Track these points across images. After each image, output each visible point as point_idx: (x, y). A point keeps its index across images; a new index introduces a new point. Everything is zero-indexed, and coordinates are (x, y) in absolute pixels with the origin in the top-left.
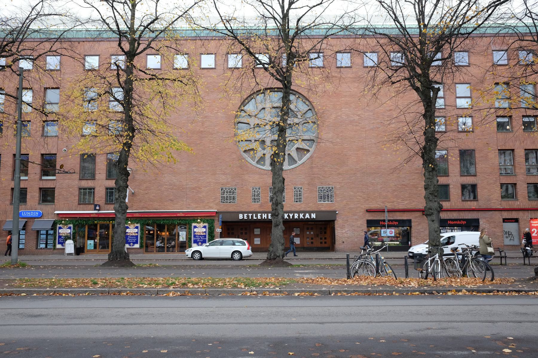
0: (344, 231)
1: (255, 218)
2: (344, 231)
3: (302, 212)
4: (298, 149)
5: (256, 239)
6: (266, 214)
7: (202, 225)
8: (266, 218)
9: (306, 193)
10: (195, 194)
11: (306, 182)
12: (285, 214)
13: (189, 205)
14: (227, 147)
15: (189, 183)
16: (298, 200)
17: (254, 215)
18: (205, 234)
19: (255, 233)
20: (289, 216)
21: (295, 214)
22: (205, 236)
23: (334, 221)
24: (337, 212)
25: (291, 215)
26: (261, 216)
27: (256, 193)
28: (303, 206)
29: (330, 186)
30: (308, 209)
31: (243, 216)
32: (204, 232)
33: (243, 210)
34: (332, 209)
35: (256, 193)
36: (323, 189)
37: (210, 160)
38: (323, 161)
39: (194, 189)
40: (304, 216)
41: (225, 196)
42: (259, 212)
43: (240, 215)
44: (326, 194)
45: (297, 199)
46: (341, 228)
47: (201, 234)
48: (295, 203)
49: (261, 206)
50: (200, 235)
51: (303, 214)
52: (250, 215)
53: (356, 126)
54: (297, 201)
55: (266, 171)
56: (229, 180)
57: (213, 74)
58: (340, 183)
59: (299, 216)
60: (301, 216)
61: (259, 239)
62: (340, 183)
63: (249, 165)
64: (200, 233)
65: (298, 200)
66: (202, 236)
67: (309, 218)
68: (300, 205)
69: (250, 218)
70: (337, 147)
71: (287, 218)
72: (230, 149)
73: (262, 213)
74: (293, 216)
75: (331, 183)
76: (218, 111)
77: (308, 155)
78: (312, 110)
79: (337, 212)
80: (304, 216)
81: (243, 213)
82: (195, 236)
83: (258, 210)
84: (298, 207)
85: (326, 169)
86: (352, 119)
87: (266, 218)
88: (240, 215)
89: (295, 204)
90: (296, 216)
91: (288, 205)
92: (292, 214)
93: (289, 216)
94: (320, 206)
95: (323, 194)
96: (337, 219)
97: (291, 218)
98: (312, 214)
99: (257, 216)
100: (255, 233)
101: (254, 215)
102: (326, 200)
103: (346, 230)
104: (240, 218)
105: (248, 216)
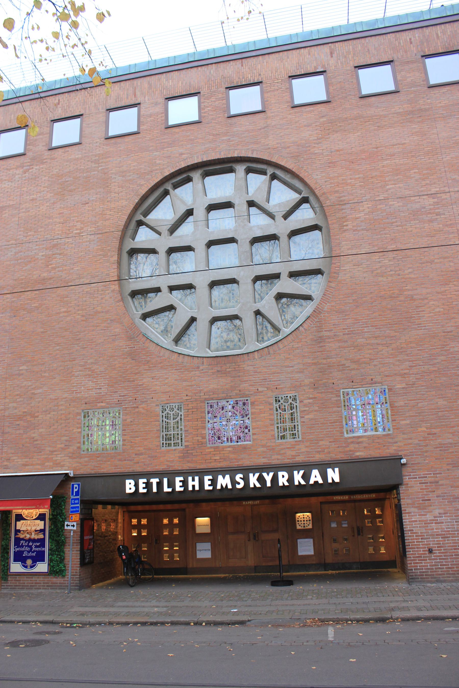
0: (429, 517)
1: (166, 489)
2: (429, 517)
3: (298, 467)
4: (279, 296)
5: (200, 546)
6: (197, 478)
7: (35, 512)
8: (197, 488)
9: (308, 413)
10: (21, 432)
11: (307, 381)
12: (251, 475)
13: (8, 460)
14: (99, 309)
15: (11, 405)
17: (165, 481)
18: (41, 536)
20: (261, 479)
21: (280, 474)
22: (42, 541)
23: (396, 487)
24: (403, 461)
25: (268, 478)
26: (185, 483)
28: (304, 449)
30: (318, 458)
31: (137, 485)
32: (41, 531)
33: (138, 469)
37: (58, 344)
38: (349, 321)
39: (20, 418)
40: (306, 477)
42: (179, 474)
43: (128, 481)
45: (285, 430)
46: (419, 508)
47: (34, 536)
48: (280, 441)
49: (186, 454)
50: (30, 540)
51: (302, 472)
52: (154, 481)
53: (431, 221)
54: (283, 437)
56: (104, 390)
57: (75, 153)
58: (403, 375)
59: (291, 479)
60: (298, 478)
61: (208, 546)
62: (403, 375)
63: (152, 347)
64: (30, 533)
66: (34, 541)
67: (321, 481)
68: (292, 447)
69: (155, 490)
70: (384, 279)
71: (258, 485)
72: (107, 312)
73: (186, 474)
74: (275, 479)
75: (378, 378)
76: (82, 228)
78: (311, 199)
79: (403, 461)
80: (306, 477)
81: (136, 476)
82: (18, 541)
83: (178, 466)
84: (290, 453)
85: (361, 341)
86: (417, 206)
87: (197, 488)
88: (128, 481)
89: (281, 444)
90: (283, 480)
91: (261, 449)
92: (271, 474)
93: (261, 479)
94: (352, 447)
96: (406, 479)
97: (269, 484)
98: (330, 471)
99: (171, 484)
101: (165, 481)
103: (436, 512)
104: (128, 491)
105: (148, 485)
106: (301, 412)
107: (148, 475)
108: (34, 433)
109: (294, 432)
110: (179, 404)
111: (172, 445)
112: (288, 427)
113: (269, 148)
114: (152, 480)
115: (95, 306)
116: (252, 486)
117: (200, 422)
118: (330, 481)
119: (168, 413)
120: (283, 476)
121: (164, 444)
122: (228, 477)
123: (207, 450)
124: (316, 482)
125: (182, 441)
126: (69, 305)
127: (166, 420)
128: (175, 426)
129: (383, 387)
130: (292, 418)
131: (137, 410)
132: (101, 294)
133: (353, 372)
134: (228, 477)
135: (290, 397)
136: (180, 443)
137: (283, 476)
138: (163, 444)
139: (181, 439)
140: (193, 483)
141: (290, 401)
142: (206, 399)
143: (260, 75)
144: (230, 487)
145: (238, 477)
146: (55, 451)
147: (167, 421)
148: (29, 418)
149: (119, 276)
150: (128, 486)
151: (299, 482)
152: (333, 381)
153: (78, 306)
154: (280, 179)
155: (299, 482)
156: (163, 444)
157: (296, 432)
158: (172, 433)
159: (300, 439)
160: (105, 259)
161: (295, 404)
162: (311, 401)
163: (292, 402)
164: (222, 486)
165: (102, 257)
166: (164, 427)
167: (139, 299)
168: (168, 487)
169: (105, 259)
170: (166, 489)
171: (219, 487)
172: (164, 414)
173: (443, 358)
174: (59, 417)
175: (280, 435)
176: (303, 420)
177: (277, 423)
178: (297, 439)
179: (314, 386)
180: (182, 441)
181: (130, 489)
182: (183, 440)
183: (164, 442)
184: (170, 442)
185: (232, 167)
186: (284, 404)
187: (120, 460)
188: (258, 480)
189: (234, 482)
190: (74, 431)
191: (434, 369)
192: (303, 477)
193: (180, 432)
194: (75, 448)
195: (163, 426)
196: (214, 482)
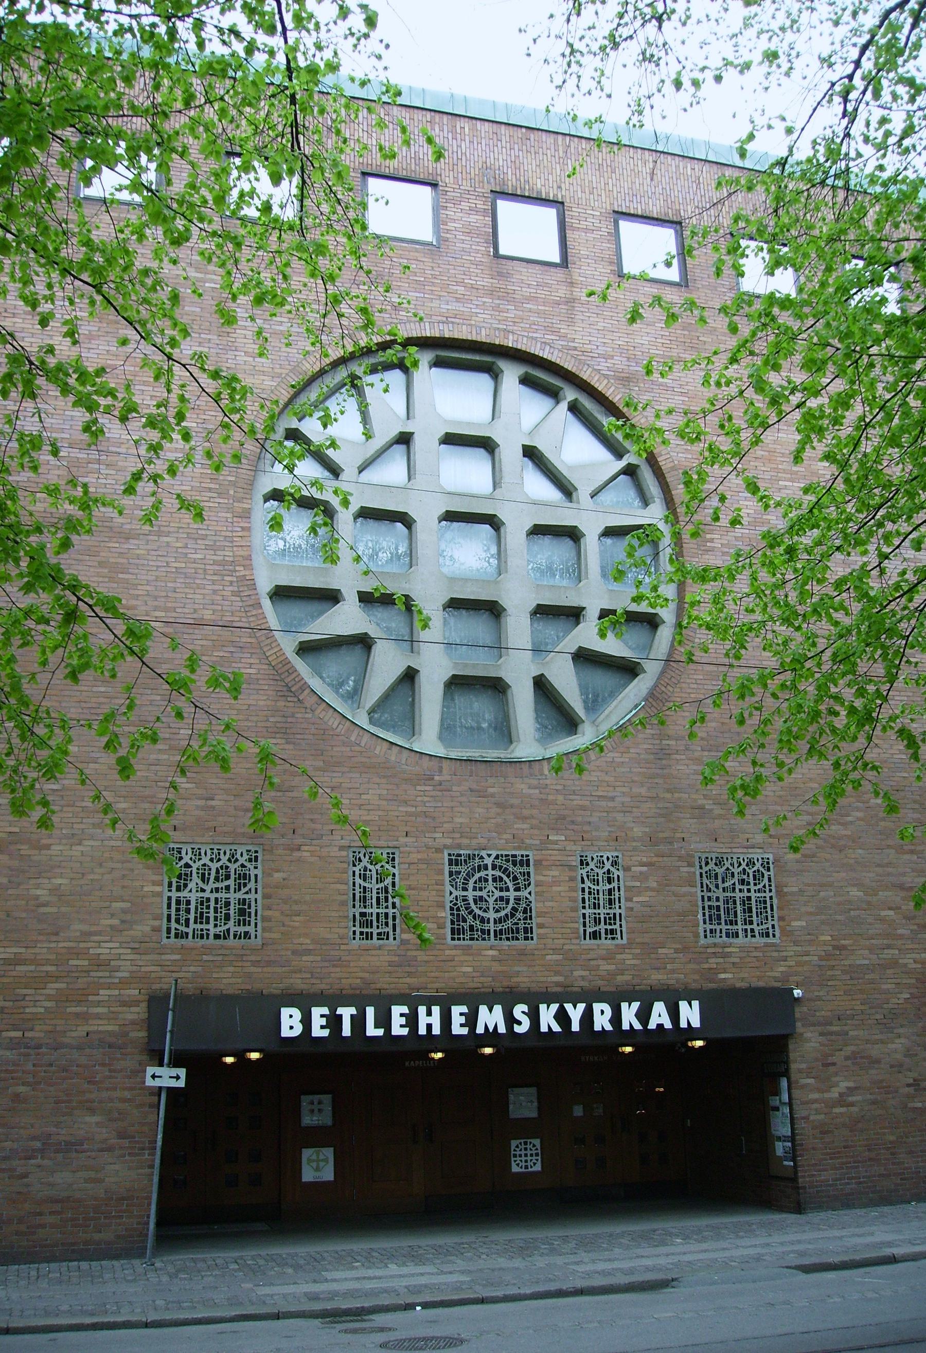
1: (372, 1031)
6: (436, 1010)
8: (436, 1031)
9: (639, 891)
11: (638, 831)
16: (602, 927)
17: (370, 1012)
19: (307, 1120)
20: (562, 1017)
21: (597, 1007)
25: (575, 1013)
26: (412, 1020)
27: (373, 886)
29: (756, 855)
30: (657, 978)
31: (307, 1021)
33: (298, 983)
34: (771, 976)
35: (373, 886)
36: (720, 871)
40: (644, 1015)
41: (194, 897)
42: (400, 999)
43: (285, 1012)
44: (738, 895)
45: (597, 921)
51: (636, 1005)
52: (347, 1013)
54: (595, 935)
55: (425, 762)
59: (616, 1019)
65: (602, 927)
67: (668, 1025)
68: (609, 957)
69: (347, 1031)
71: (556, 1028)
74: (588, 1017)
77: (638, 688)
80: (644, 1015)
83: (386, 983)
84: (606, 967)
87: (436, 1031)
88: (285, 1012)
92: (581, 1007)
93: (562, 1017)
95: (722, 896)
97: (575, 1027)
98: (683, 1005)
99: (384, 1020)
100: (307, 1120)
101: (370, 1012)
102: (740, 927)
104: (285, 1033)
105: (334, 1022)
106: (628, 889)
107: (333, 1000)
108: (38, 886)
109: (613, 927)
110: (390, 851)
111: (375, 936)
112: (602, 917)
113: (575, 349)
114: (340, 1011)
115: (196, 606)
116: (544, 1028)
117: (434, 893)
118: (683, 1024)
119: (365, 869)
120: (602, 1012)
121: (358, 933)
122: (498, 1009)
123: (447, 952)
124: (660, 1026)
125: (394, 930)
126: (132, 592)
127: (361, 882)
128: (382, 896)
129: (766, 856)
130: (610, 900)
131: (297, 854)
132: (214, 582)
133: (717, 823)
134: (498, 1009)
135: (608, 859)
136: (391, 933)
137: (602, 1012)
138: (354, 932)
139: (394, 925)
140: (429, 1020)
141: (608, 866)
142: (446, 847)
143: (559, 187)
144: (502, 1029)
145: (519, 1011)
146: (91, 934)
147: (363, 884)
148: (25, 849)
149: (670, 654)
150: (285, 1022)
151: (631, 1025)
152: (683, 835)
153: (156, 598)
154: (580, 413)
155: (631, 1025)
156: (354, 932)
157: (617, 927)
158: (375, 910)
159: (625, 941)
160: (221, 501)
161: (616, 873)
162: (644, 869)
163: (612, 869)
164: (486, 1027)
165: (215, 495)
166: (357, 898)
167: (297, 610)
168: (376, 1027)
169: (221, 501)
170: (372, 1031)
171: (480, 1030)
172: (357, 869)
173: (860, 814)
174: (107, 855)
175: (589, 930)
176: (630, 904)
177: (584, 908)
178: (619, 941)
179: (651, 840)
180: (394, 930)
181: (291, 1028)
182: (398, 929)
183: (358, 930)
184: (369, 930)
185: (493, 363)
186: (596, 870)
187: (255, 963)
188: (556, 1017)
189: (511, 1020)
190: (146, 889)
191: (845, 832)
192: (637, 1015)
193: (391, 911)
194: (148, 929)
195: (354, 895)
196: (471, 1019)
